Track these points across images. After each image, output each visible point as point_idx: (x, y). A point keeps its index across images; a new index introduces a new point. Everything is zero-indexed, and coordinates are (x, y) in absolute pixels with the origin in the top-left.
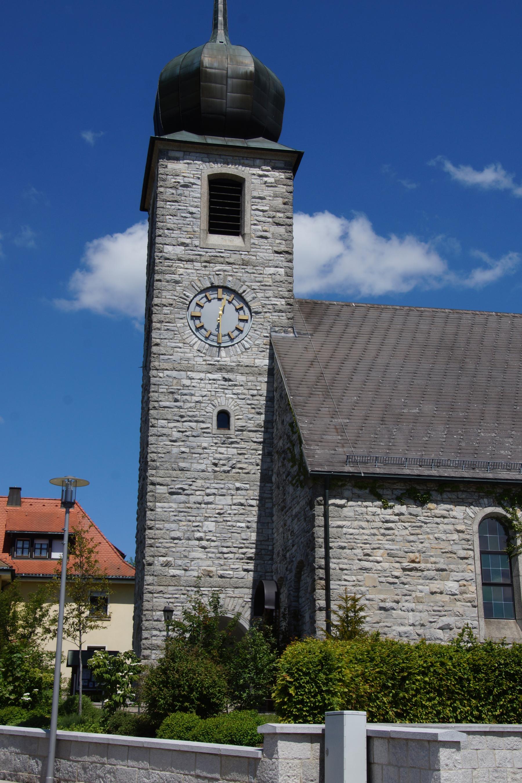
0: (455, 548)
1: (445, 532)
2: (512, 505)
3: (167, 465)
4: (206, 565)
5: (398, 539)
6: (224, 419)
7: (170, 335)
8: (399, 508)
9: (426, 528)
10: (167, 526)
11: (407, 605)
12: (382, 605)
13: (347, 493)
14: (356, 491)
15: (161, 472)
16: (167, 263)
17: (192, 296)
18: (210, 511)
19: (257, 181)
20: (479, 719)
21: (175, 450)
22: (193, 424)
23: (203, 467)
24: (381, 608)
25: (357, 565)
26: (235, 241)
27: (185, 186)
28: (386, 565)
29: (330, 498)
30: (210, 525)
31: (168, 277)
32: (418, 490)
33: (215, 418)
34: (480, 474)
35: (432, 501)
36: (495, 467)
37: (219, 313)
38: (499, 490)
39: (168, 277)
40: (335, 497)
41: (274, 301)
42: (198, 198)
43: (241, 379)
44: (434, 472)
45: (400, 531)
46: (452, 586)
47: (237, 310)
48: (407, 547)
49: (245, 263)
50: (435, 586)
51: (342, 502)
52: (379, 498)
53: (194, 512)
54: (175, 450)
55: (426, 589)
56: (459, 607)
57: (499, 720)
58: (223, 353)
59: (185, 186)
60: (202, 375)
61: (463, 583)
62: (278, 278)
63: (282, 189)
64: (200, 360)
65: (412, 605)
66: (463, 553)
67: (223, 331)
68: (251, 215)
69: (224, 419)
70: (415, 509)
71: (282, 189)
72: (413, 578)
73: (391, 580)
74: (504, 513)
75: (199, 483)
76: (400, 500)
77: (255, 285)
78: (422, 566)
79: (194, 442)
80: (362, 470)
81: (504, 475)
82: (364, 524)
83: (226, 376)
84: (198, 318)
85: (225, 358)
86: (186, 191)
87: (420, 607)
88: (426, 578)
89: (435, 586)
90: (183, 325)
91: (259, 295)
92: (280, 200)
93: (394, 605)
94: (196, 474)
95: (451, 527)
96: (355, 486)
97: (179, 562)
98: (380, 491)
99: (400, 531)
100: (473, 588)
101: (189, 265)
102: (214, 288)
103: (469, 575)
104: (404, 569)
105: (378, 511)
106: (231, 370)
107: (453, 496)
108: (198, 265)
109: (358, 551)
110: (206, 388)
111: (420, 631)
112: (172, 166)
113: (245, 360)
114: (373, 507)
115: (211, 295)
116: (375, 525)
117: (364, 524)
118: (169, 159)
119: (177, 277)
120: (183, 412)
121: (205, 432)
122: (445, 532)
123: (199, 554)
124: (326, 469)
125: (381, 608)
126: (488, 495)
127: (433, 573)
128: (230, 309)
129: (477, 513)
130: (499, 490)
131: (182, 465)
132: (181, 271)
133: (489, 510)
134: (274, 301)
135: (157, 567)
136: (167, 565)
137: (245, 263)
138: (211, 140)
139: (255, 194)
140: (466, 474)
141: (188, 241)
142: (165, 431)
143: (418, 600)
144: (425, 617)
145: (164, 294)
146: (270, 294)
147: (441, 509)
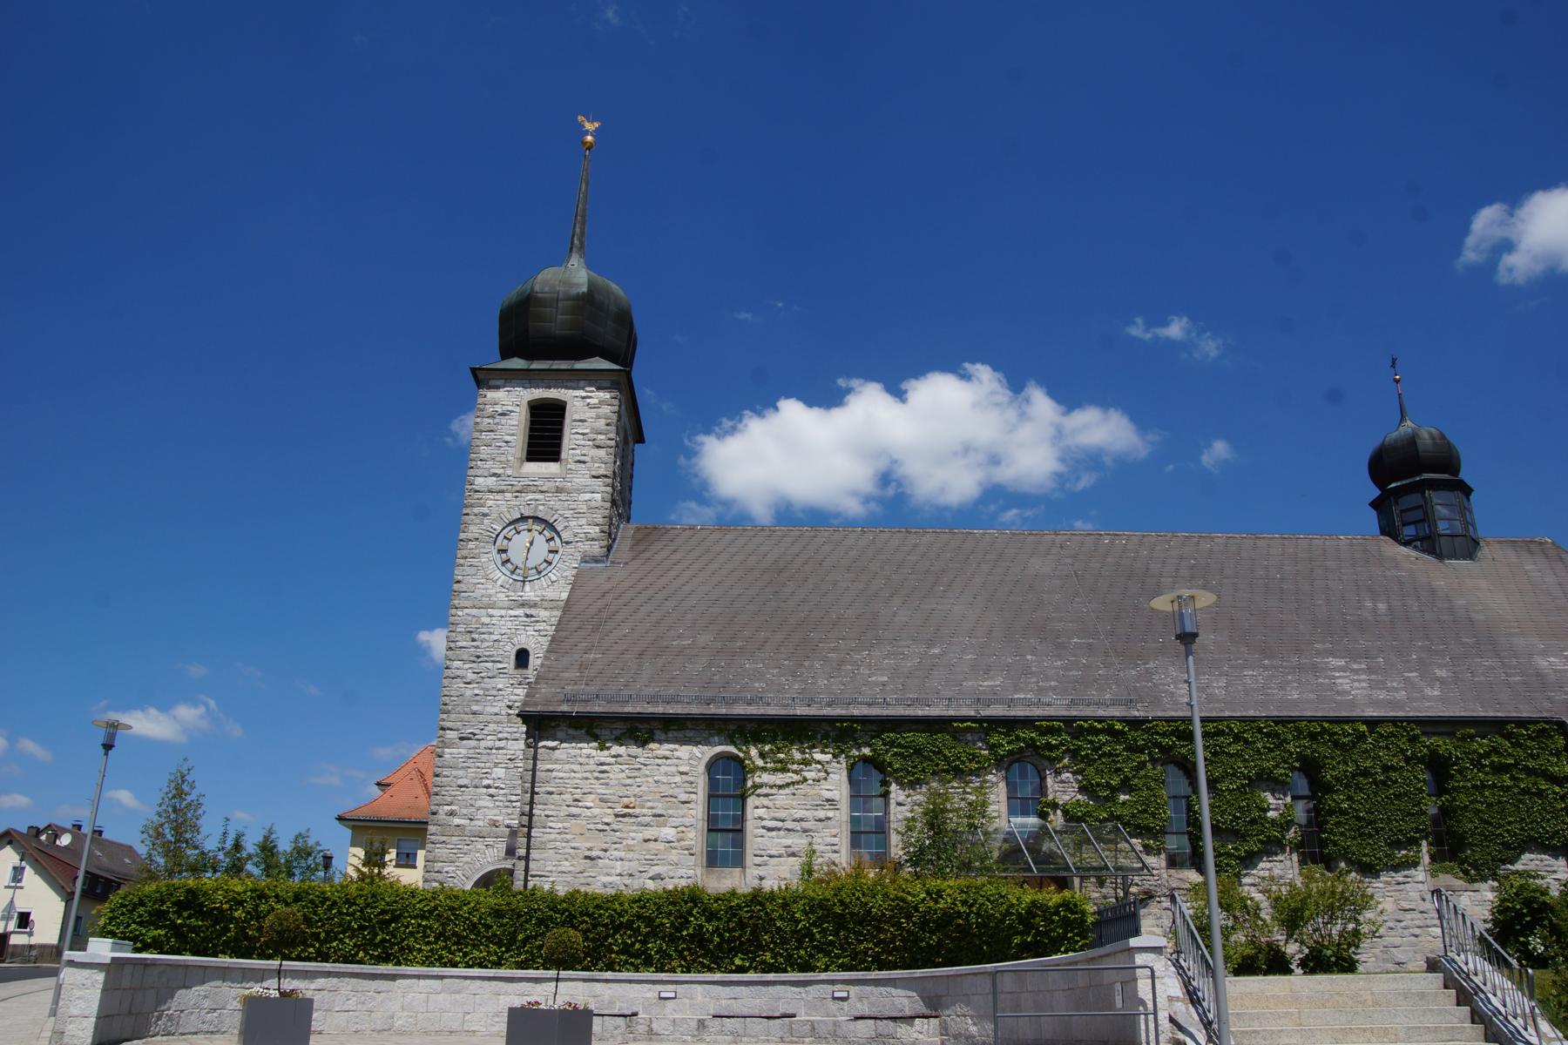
0: (676, 791)
1: (666, 774)
2: (746, 743)
3: (459, 709)
4: (492, 815)
5: (613, 782)
6: (522, 657)
7: (473, 571)
8: (616, 749)
9: (645, 770)
10: (455, 772)
11: (616, 853)
12: (588, 853)
13: (560, 734)
14: (571, 732)
15: (453, 716)
16: (477, 495)
17: (499, 529)
18: (500, 757)
19: (579, 403)
20: (498, 964)
21: (468, 693)
22: (489, 665)
23: (496, 710)
24: (587, 857)
25: (565, 810)
26: (551, 468)
27: (503, 414)
28: (596, 811)
29: (541, 739)
30: (499, 772)
31: (476, 510)
32: (640, 729)
33: (513, 657)
34: (713, 710)
35: (654, 741)
36: (735, 701)
37: (527, 546)
38: (732, 727)
39: (476, 510)
40: (547, 739)
41: (588, 529)
42: (515, 427)
43: (543, 614)
44: (660, 709)
45: (616, 774)
46: (668, 832)
47: (548, 541)
48: (624, 791)
49: (559, 490)
50: (650, 833)
51: (555, 744)
52: (595, 738)
53: (484, 758)
54: (468, 693)
55: (640, 836)
56: (674, 856)
57: (522, 965)
58: (527, 587)
59: (503, 414)
60: (503, 612)
61: (681, 828)
62: (593, 504)
63: (606, 410)
64: (502, 596)
65: (622, 854)
66: (684, 797)
67: (530, 564)
68: (572, 440)
69: (522, 657)
70: (634, 750)
71: (606, 410)
72: (625, 825)
73: (601, 827)
74: (735, 751)
75: (492, 727)
76: (619, 740)
77: (568, 513)
78: (637, 811)
79: (489, 683)
80: (576, 709)
81: (740, 710)
82: (576, 767)
83: (529, 612)
84: (505, 551)
85: (529, 593)
86: (503, 420)
87: (630, 855)
88: (641, 824)
89: (650, 833)
90: (489, 559)
91: (572, 524)
92: (603, 421)
93: (601, 854)
94: (489, 718)
95: (673, 769)
96: (570, 726)
97: (465, 811)
98: (597, 731)
99: (616, 774)
100: (692, 835)
101: (499, 497)
102: (523, 519)
103: (688, 821)
104: (617, 816)
105: (594, 752)
106: (534, 605)
107: (680, 735)
108: (508, 495)
109: (567, 797)
110: (506, 626)
111: (628, 882)
112: (491, 395)
113: (550, 594)
114: (588, 749)
115: (522, 526)
116: (587, 768)
117: (576, 767)
118: (489, 388)
119: (485, 510)
120: (479, 652)
121: (501, 672)
122: (666, 774)
123: (486, 802)
124: (539, 708)
125: (587, 857)
126: (719, 732)
127: (648, 819)
128: (540, 541)
129: (702, 753)
130: (732, 727)
131: (475, 708)
132: (490, 503)
133: (719, 749)
134: (588, 529)
135: (441, 816)
136: (452, 814)
137: (559, 490)
138: (537, 365)
139: (576, 417)
140: (695, 710)
141: (499, 471)
142: (459, 673)
143: (629, 849)
144: (634, 866)
145: (471, 528)
146: (583, 521)
147: (664, 749)
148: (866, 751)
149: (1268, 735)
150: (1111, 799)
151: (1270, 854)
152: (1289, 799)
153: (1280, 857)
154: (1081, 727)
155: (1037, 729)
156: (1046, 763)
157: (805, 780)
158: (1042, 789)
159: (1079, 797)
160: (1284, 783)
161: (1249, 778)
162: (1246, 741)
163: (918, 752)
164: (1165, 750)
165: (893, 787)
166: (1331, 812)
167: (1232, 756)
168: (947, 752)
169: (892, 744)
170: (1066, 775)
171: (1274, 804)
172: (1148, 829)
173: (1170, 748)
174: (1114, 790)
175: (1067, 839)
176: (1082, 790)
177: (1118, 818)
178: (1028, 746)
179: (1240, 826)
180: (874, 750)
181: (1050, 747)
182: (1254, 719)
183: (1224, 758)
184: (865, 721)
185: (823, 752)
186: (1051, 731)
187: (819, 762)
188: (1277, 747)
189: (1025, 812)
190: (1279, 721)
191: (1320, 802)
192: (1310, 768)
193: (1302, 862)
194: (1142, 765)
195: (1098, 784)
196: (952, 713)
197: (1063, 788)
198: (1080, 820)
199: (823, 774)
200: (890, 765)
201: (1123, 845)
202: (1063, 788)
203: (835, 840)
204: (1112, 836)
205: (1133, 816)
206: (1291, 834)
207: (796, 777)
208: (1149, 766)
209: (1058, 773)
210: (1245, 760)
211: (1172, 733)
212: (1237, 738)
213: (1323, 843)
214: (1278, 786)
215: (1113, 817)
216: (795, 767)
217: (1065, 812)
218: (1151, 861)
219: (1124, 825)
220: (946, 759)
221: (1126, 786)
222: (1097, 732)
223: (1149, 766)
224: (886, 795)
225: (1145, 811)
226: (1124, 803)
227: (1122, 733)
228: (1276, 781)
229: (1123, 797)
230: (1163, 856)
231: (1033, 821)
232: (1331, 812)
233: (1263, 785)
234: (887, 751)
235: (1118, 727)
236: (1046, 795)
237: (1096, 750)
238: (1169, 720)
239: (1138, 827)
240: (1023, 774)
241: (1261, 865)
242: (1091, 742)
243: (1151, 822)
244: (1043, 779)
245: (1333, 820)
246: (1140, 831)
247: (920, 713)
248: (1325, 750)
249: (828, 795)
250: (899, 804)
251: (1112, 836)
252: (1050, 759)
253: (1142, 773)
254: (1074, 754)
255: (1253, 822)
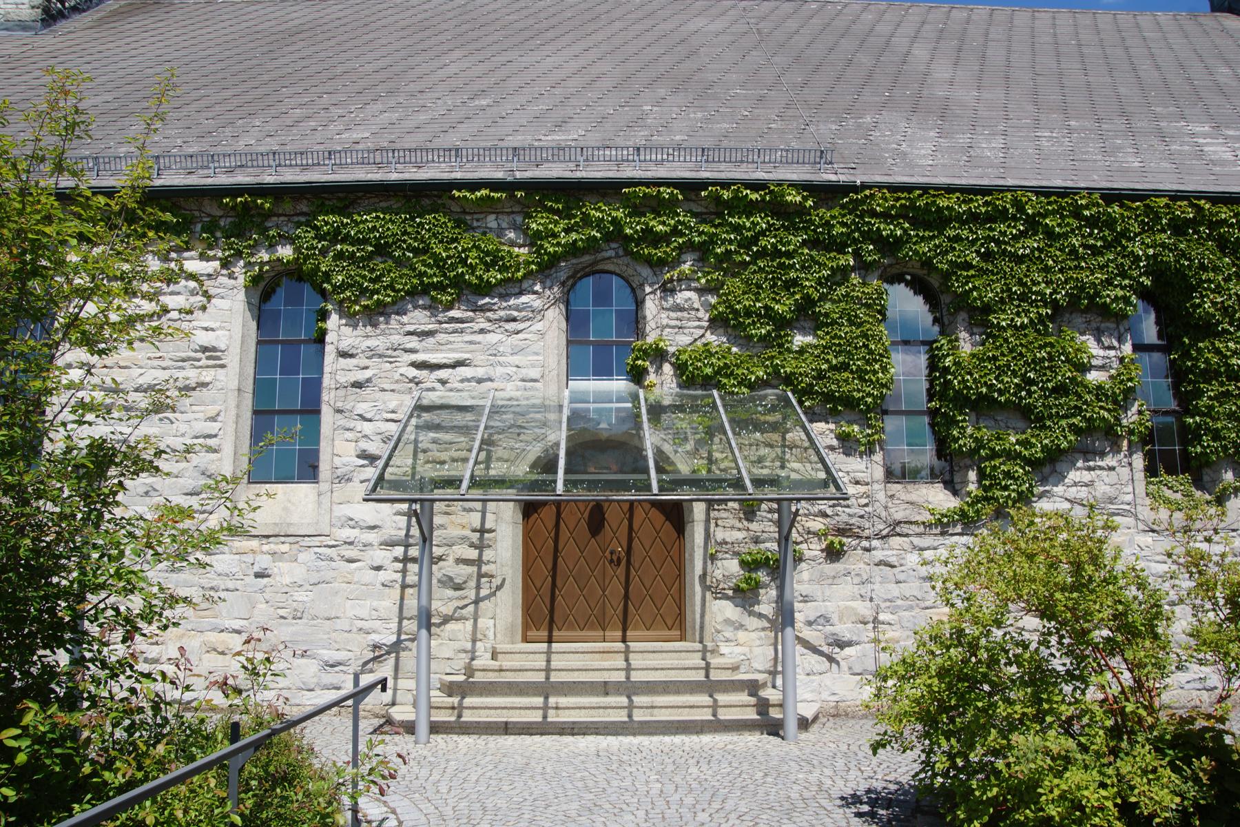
148: (286, 252)
149: (1092, 222)
150: (776, 342)
151: (1088, 453)
152: (1127, 348)
153: (1109, 461)
154: (718, 199)
155: (626, 201)
156: (646, 271)
157: (166, 311)
158: (636, 322)
159: (714, 339)
160: (1121, 317)
161: (1055, 304)
162: (1050, 234)
163: (382, 250)
164: (889, 246)
165: (334, 321)
166: (1209, 375)
167: (1019, 260)
168: (438, 249)
169: (335, 236)
170: (685, 296)
171: (1102, 357)
172: (850, 403)
173: (898, 243)
174: (782, 324)
175: (682, 422)
176: (717, 322)
177: (788, 380)
178: (608, 237)
179: (1035, 398)
180: (297, 250)
181: (656, 239)
182: (1064, 193)
183: (1006, 266)
184: (279, 192)
185: (203, 257)
186: (658, 206)
187: (192, 277)
188: (1108, 246)
189: (603, 370)
190: (1111, 196)
191: (1186, 355)
192: (1169, 293)
193: (1151, 471)
194: (841, 275)
195: (748, 313)
196: (458, 175)
197: (677, 320)
198: (708, 382)
199: (199, 299)
200: (327, 276)
201: (796, 435)
202: (677, 320)
203: (212, 427)
204: (777, 417)
205: (820, 376)
206: (1131, 417)
207: (148, 307)
208: (855, 278)
209: (668, 289)
210: (1047, 269)
211: (903, 214)
212: (1033, 224)
213: (1189, 435)
214: (1107, 319)
215: (778, 378)
216: (145, 287)
217: (680, 368)
218: (849, 467)
219: (802, 394)
220: (439, 263)
221: (807, 314)
222: (750, 208)
223: (855, 278)
224: (320, 339)
225: (844, 367)
226: (802, 351)
227: (800, 210)
228: (1104, 311)
229: (799, 340)
230: (878, 457)
231: (620, 385)
232: (1209, 375)
233: (1079, 320)
234: (324, 252)
235: (793, 197)
236: (640, 332)
237: (746, 244)
238: (894, 188)
239: (828, 397)
240: (602, 298)
241: (1073, 476)
242: (737, 229)
243: (852, 387)
244: (639, 303)
245: (1212, 389)
246: (835, 406)
247: (394, 176)
248: (1206, 253)
249: (203, 338)
250: (344, 355)
251: (777, 417)
252: (648, 261)
253: (842, 291)
254: (703, 251)
255: (1061, 390)
